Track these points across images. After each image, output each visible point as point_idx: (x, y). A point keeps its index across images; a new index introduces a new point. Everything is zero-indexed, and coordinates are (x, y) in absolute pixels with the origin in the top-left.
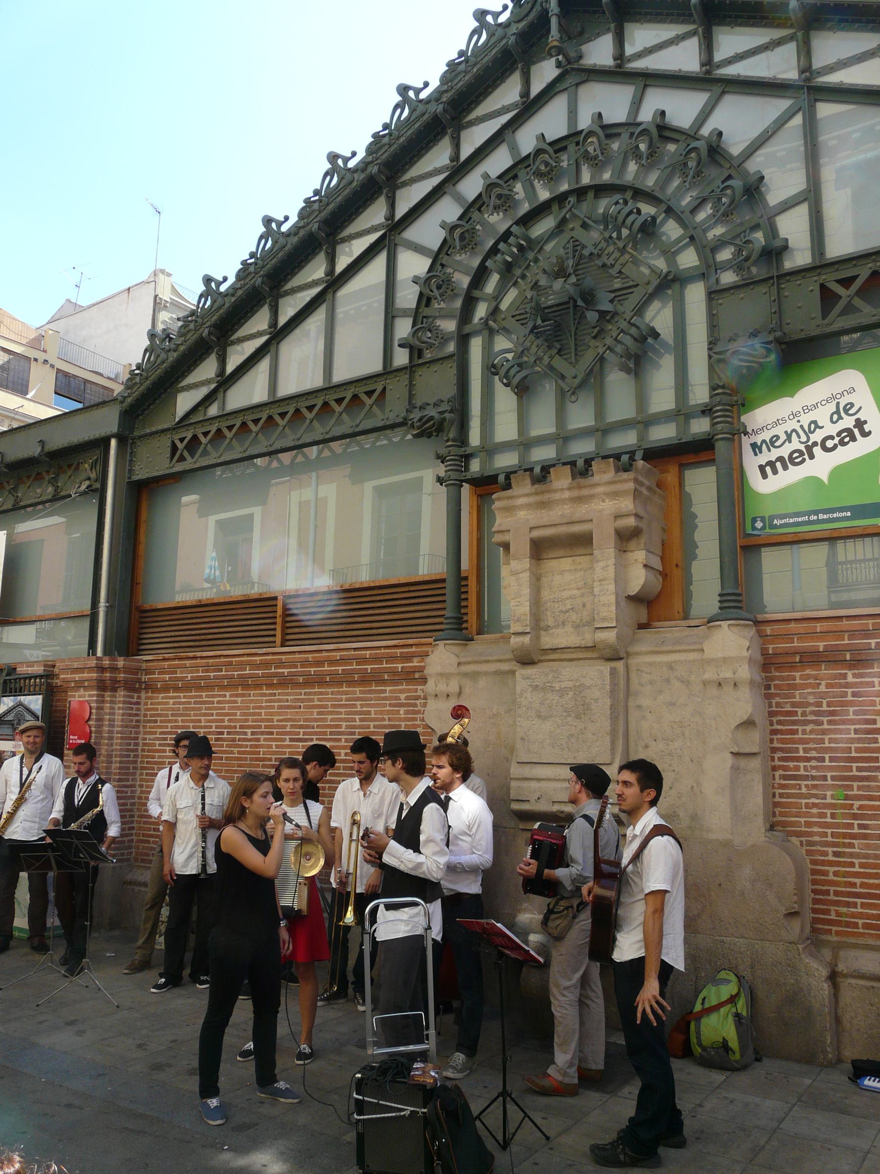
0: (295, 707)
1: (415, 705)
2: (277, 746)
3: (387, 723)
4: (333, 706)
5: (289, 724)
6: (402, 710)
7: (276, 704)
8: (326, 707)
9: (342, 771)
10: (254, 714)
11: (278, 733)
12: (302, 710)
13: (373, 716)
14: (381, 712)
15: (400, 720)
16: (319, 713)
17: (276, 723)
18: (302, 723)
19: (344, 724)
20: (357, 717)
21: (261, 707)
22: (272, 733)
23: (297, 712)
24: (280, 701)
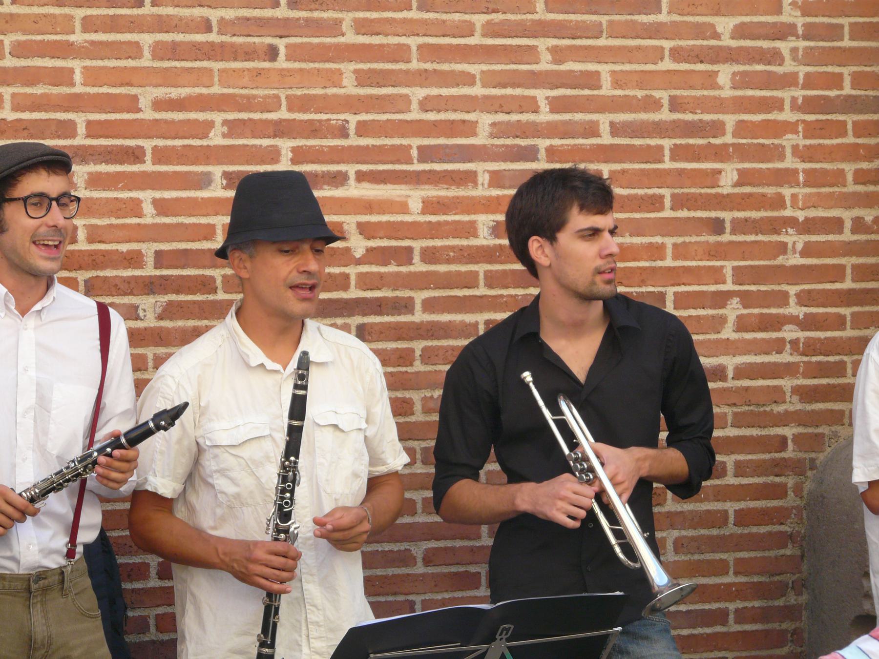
0: (249, 54)
1: (775, 57)
2: (162, 207)
3: (665, 115)
4: (429, 52)
5: (218, 117)
6: (725, 73)
7: (147, 39)
8: (400, 53)
9: (482, 291)
10: (31, 77)
11: (161, 155)
12: (282, 63)
13: (607, 90)
14: (644, 80)
15: (720, 105)
16: (363, 79)
17: (148, 114)
18: (283, 114)
19: (485, 120)
20: (541, 95)
21: (66, 50)
22: (136, 155)
23: (259, 73)
24: (162, 24)
